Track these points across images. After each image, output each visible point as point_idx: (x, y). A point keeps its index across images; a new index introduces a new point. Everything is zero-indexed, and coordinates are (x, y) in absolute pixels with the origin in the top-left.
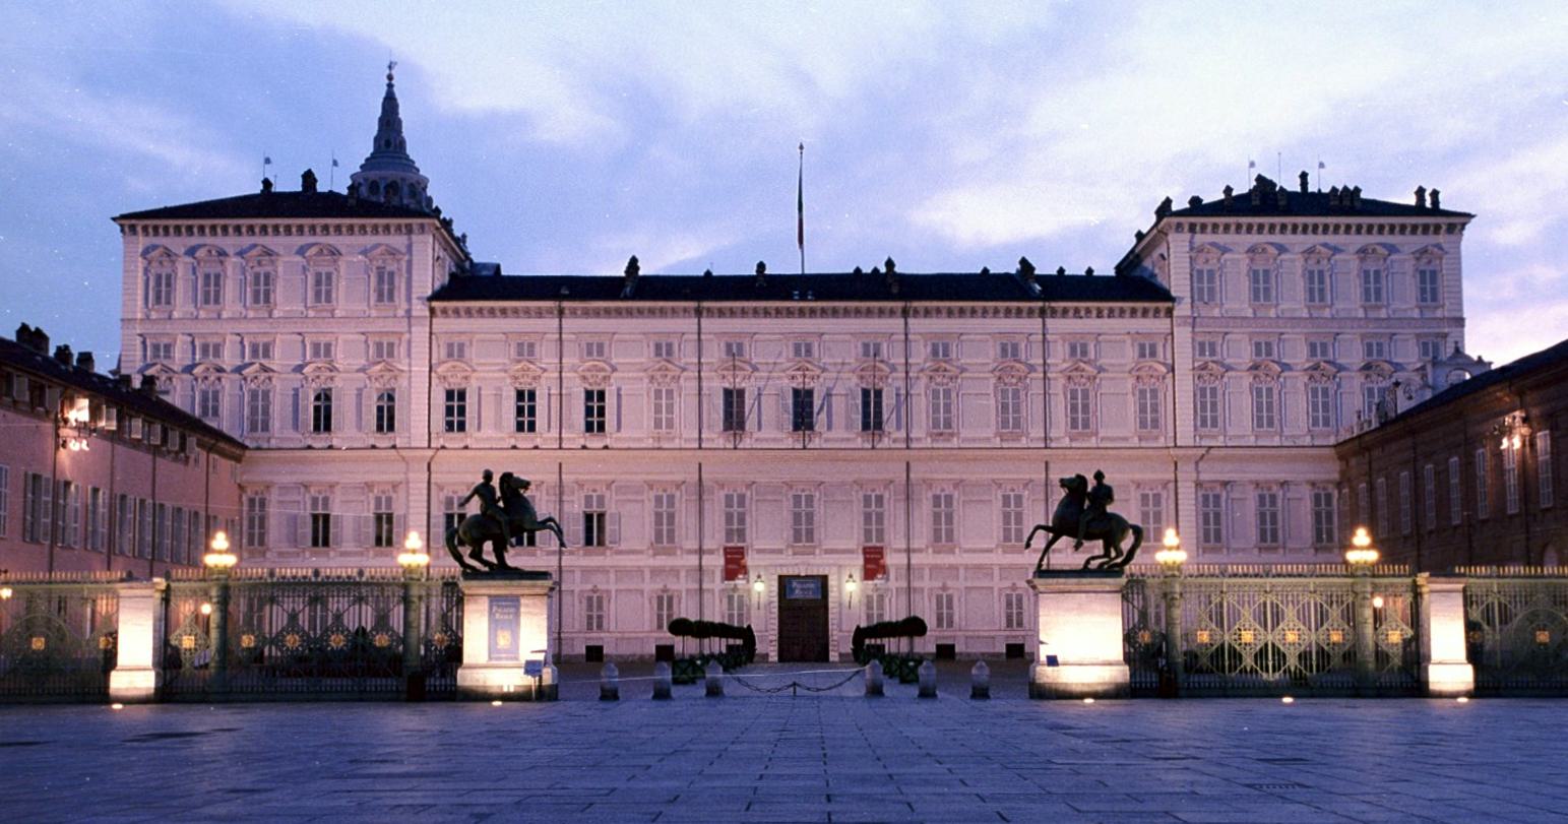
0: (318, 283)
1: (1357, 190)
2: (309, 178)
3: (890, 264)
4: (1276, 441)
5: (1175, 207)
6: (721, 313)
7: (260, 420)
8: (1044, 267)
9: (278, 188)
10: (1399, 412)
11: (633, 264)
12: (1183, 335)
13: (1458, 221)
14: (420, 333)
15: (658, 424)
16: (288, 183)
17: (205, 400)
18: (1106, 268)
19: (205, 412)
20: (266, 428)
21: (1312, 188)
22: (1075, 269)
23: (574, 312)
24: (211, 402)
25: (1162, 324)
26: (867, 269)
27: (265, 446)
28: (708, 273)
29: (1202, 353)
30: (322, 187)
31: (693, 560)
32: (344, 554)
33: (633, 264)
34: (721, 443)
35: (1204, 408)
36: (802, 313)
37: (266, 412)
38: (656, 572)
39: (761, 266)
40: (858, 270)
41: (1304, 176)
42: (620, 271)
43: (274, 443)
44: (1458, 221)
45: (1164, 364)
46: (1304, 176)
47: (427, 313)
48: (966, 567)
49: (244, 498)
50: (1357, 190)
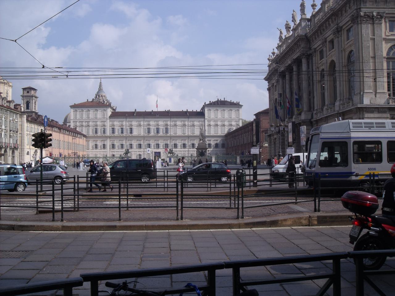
0: (95, 114)
3: (169, 110)
5: (206, 104)
6: (147, 118)
7: (88, 132)
8: (190, 110)
9: (89, 101)
11: (136, 110)
12: (206, 121)
13: (241, 106)
14: (108, 121)
15: (139, 132)
17: (81, 130)
18: (199, 110)
19: (81, 131)
20: (89, 133)
21: (225, 100)
22: (195, 110)
23: (128, 118)
24: (82, 130)
25: (203, 120)
26: (167, 111)
28: (145, 111)
31: (143, 150)
33: (136, 110)
34: (147, 135)
36: (157, 118)
37: (89, 131)
38: (139, 151)
40: (166, 110)
41: (224, 98)
42: (134, 111)
44: (241, 106)
46: (224, 98)
48: (178, 151)
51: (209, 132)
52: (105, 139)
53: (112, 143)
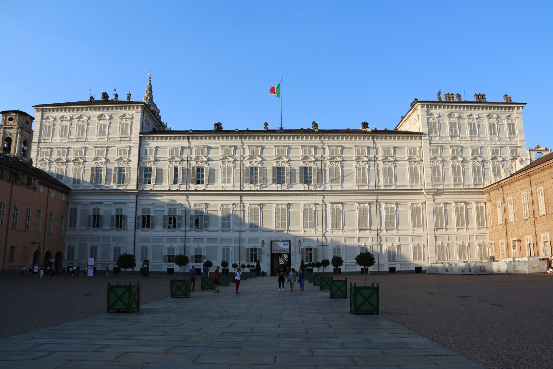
1: (483, 96)
2: (105, 95)
4: (462, 187)
10: (518, 170)
16: (98, 97)
27: (78, 189)
29: (433, 153)
30: (110, 99)
32: (104, 230)
35: (435, 175)
39: (266, 125)
43: (80, 188)
45: (419, 157)
47: (138, 139)
49: (69, 208)
50: (483, 96)
51: (435, 181)
52: (125, 201)
53: (144, 210)
